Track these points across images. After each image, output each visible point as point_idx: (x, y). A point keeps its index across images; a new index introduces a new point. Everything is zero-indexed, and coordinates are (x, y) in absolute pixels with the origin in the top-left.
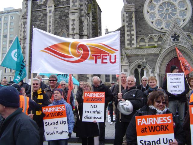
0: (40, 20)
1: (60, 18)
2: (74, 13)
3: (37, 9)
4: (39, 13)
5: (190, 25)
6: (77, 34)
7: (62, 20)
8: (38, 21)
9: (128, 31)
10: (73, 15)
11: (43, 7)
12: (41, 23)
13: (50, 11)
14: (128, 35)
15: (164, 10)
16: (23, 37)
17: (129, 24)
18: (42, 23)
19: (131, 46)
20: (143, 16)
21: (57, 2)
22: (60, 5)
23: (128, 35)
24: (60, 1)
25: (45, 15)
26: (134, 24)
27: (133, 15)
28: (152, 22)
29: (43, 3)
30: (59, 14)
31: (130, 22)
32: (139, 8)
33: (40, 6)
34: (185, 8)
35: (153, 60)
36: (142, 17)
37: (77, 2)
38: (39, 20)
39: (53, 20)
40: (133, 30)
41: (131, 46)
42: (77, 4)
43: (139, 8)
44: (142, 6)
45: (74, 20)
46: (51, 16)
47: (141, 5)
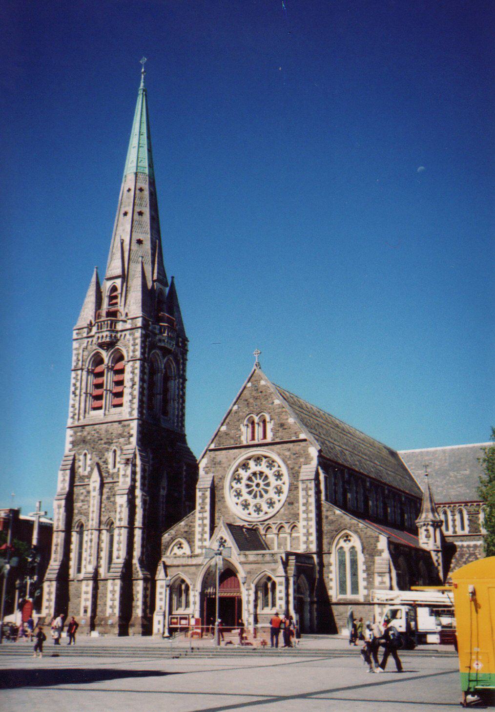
0: (83, 501)
1: (108, 498)
2: (122, 496)
3: (80, 482)
4: (81, 489)
5: (285, 510)
6: (125, 527)
7: (111, 502)
8: (79, 502)
9: (199, 519)
10: (121, 497)
11: (86, 480)
12: (83, 505)
13: (94, 490)
14: (199, 525)
15: (254, 484)
16: (57, 528)
17: (202, 508)
18: (84, 505)
19: (202, 543)
20: (223, 494)
21: (106, 473)
22: (108, 478)
23: (199, 525)
24: (109, 472)
25: (89, 492)
26: (208, 507)
27: (208, 494)
28: (237, 504)
29: (86, 473)
30: (108, 492)
31: (203, 505)
32: (219, 482)
33: (82, 478)
34: (282, 481)
35: (194, 574)
36: (222, 496)
37: (128, 476)
38: (80, 501)
39: (97, 503)
40: (206, 518)
41: (202, 543)
42: (129, 480)
43: (219, 482)
44: (222, 478)
45: (121, 506)
46: (94, 497)
47: (222, 476)
